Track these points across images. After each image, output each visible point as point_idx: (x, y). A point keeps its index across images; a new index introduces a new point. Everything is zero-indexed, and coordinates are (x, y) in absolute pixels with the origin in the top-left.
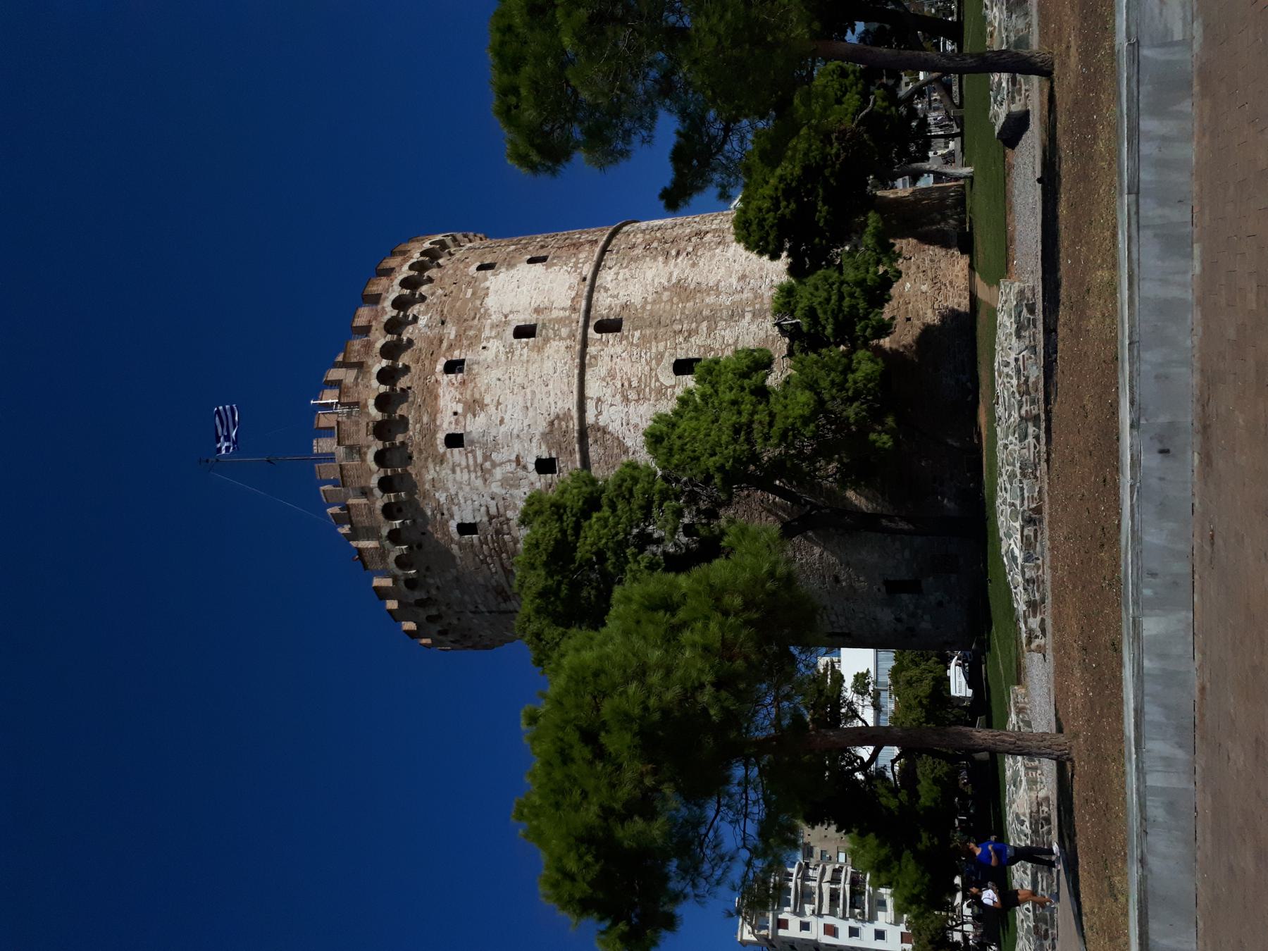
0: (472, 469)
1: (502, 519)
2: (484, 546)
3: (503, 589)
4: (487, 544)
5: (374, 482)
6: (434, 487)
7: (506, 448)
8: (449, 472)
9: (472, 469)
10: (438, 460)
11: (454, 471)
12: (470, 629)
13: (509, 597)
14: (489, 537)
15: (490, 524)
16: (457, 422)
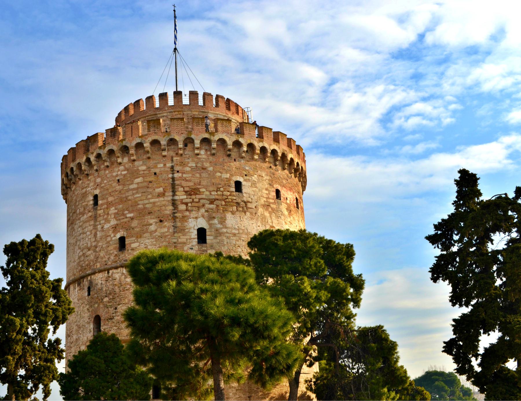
0: (268, 200)
1: (245, 208)
2: (229, 193)
3: (197, 194)
4: (230, 195)
5: (266, 145)
6: (260, 176)
7: (277, 222)
8: (266, 186)
9: (268, 200)
10: (270, 182)
11: (267, 189)
12: (149, 158)
13: (191, 195)
14: (235, 198)
15: (242, 201)
16: (284, 198)
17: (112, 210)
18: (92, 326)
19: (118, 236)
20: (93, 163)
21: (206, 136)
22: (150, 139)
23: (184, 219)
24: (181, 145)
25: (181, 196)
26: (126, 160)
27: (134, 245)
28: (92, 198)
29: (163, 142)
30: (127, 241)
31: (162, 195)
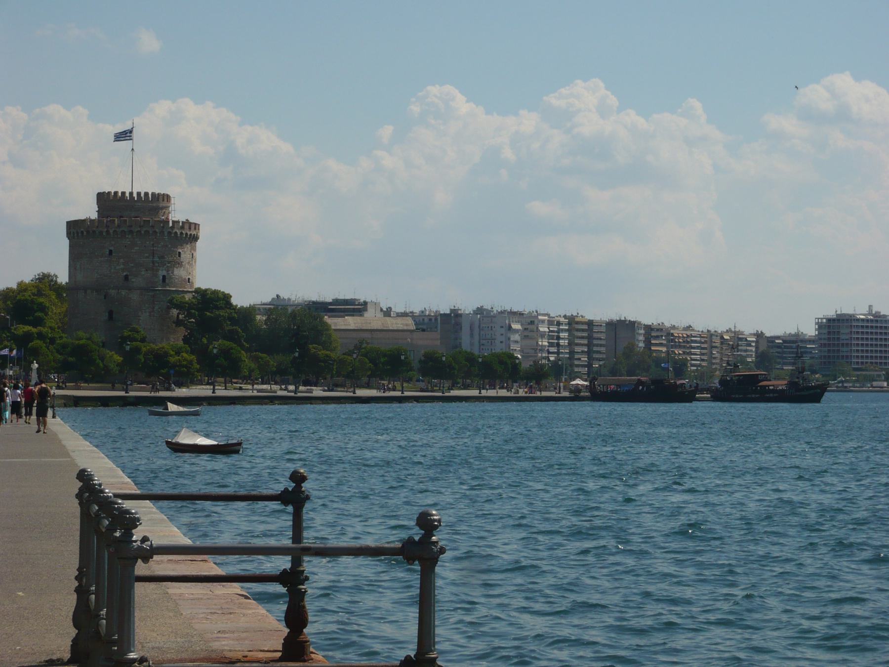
5: (191, 232)
17: (122, 260)
18: (107, 314)
19: (125, 274)
20: (112, 234)
21: (170, 230)
22: (145, 229)
23: (157, 270)
24: (159, 235)
25: (156, 259)
26: (130, 236)
27: (133, 280)
28: (108, 251)
29: (151, 232)
30: (130, 277)
31: (147, 257)
